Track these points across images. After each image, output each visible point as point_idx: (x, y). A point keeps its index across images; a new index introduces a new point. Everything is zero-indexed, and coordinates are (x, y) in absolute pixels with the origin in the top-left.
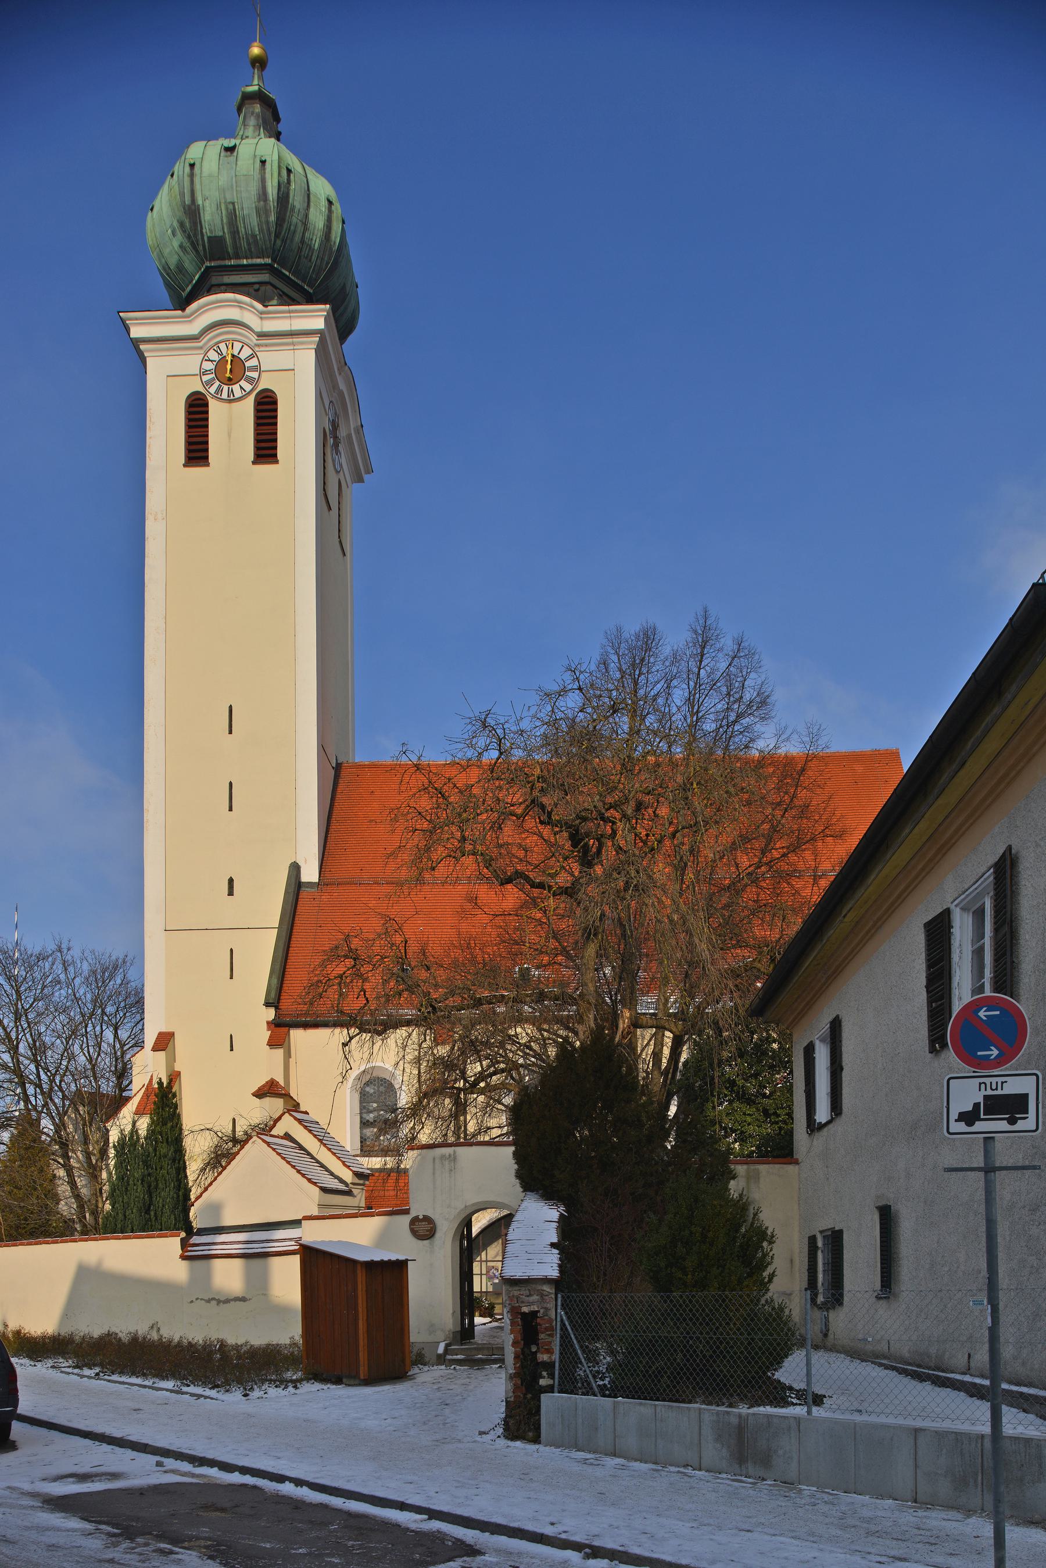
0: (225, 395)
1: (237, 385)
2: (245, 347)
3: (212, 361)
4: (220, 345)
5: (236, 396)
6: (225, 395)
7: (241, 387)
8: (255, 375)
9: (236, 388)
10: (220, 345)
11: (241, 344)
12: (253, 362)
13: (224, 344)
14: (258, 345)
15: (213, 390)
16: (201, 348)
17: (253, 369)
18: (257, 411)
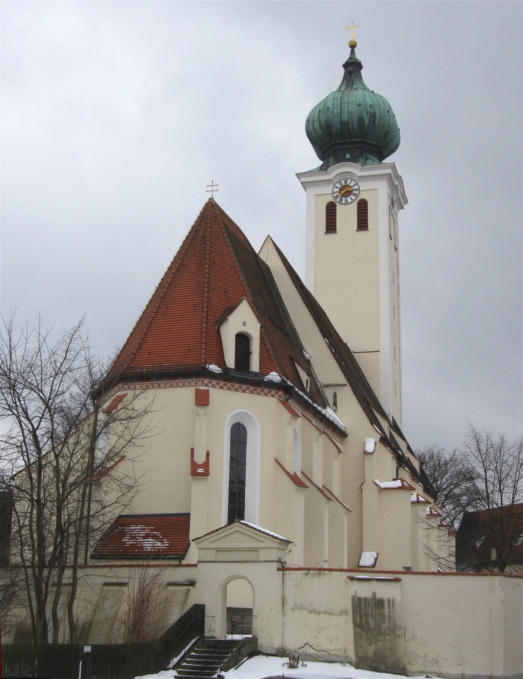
0: (343, 202)
1: (349, 197)
2: (353, 181)
3: (338, 188)
4: (341, 181)
5: (349, 202)
6: (343, 202)
7: (351, 198)
8: (357, 192)
9: (349, 199)
10: (341, 181)
11: (351, 180)
12: (357, 187)
13: (343, 180)
14: (358, 180)
15: (338, 200)
16: (333, 183)
17: (357, 190)
18: (358, 207)
